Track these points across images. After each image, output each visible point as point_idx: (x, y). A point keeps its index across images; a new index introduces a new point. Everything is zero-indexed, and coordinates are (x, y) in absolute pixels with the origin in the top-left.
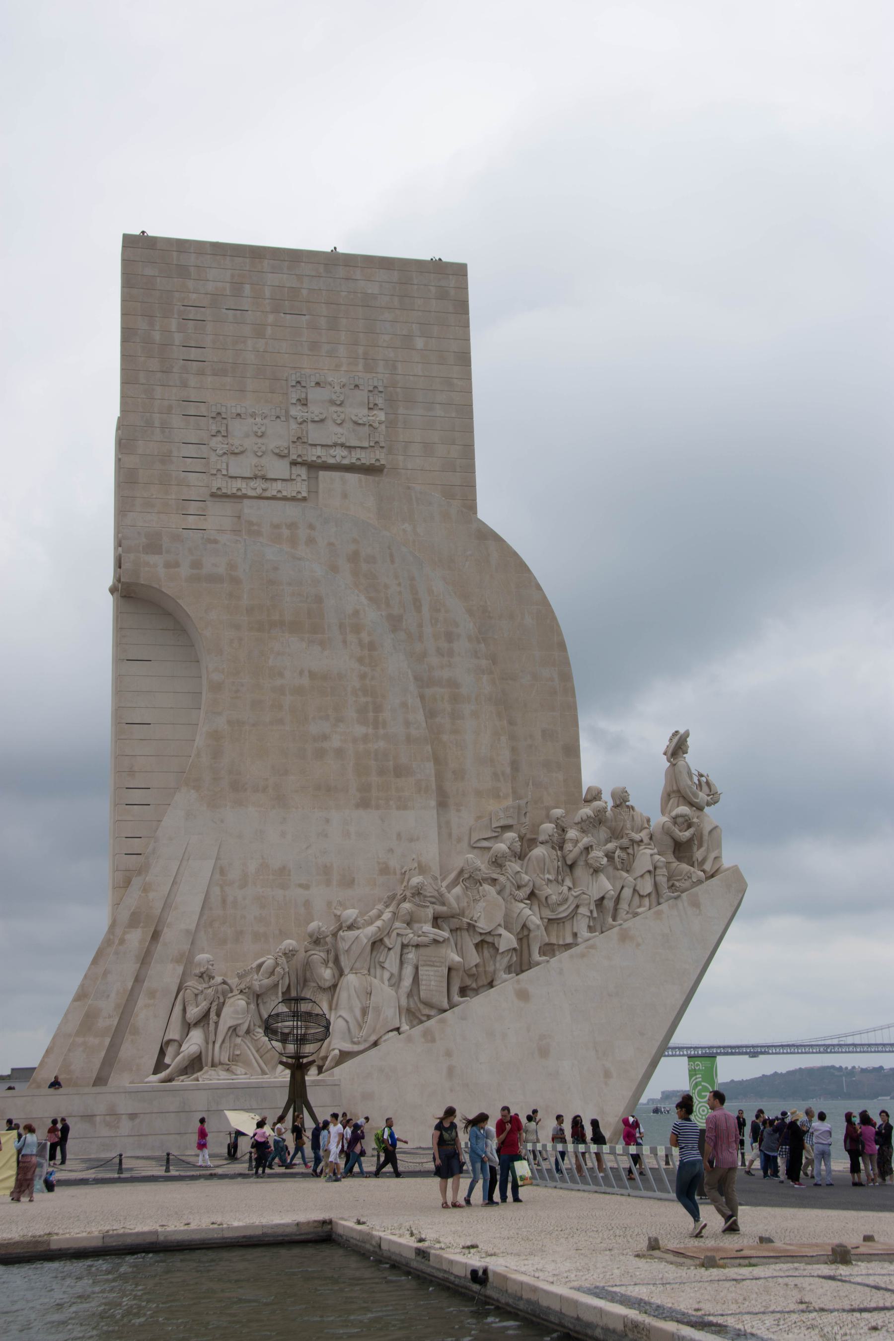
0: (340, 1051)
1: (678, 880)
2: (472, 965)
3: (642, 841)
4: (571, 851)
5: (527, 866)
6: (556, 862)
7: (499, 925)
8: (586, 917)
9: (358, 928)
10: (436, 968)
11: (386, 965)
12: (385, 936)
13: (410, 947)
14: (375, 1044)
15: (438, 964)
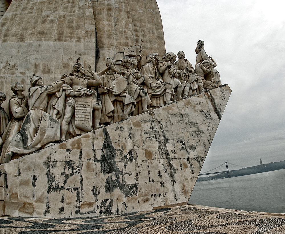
0: (13, 152)
1: (207, 86)
2: (110, 111)
3: (191, 71)
4: (162, 67)
5: (141, 72)
6: (154, 70)
7: (126, 93)
8: (169, 94)
9: (39, 86)
10: (85, 109)
11: (56, 107)
12: (57, 92)
13: (71, 98)
14: (41, 148)
15: (86, 106)
